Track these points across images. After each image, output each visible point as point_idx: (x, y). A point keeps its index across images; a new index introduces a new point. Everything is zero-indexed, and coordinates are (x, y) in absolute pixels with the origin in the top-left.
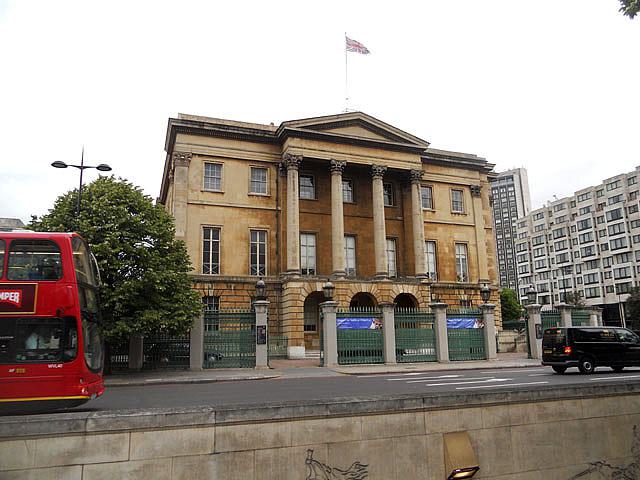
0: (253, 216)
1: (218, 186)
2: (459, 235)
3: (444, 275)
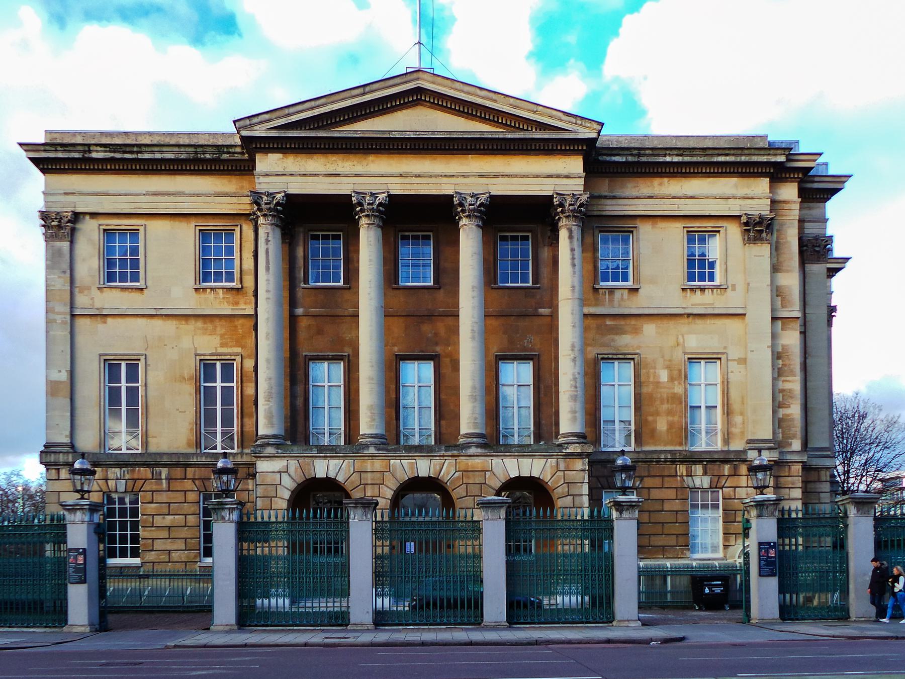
0: (205, 331)
1: (135, 277)
3: (653, 431)
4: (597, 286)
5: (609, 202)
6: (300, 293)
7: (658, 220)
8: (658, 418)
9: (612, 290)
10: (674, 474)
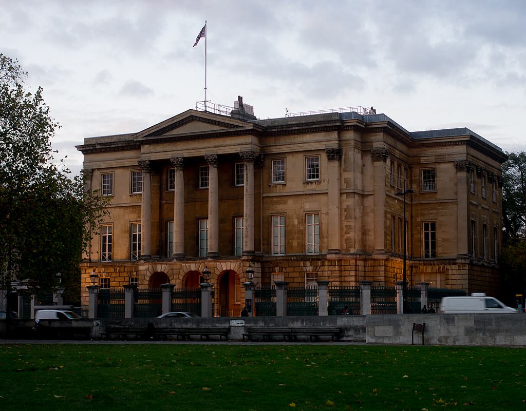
2: (308, 205)
3: (292, 246)
4: (270, 184)
5: (274, 147)
6: (164, 194)
7: (294, 153)
8: (294, 241)
9: (276, 185)
10: (298, 265)
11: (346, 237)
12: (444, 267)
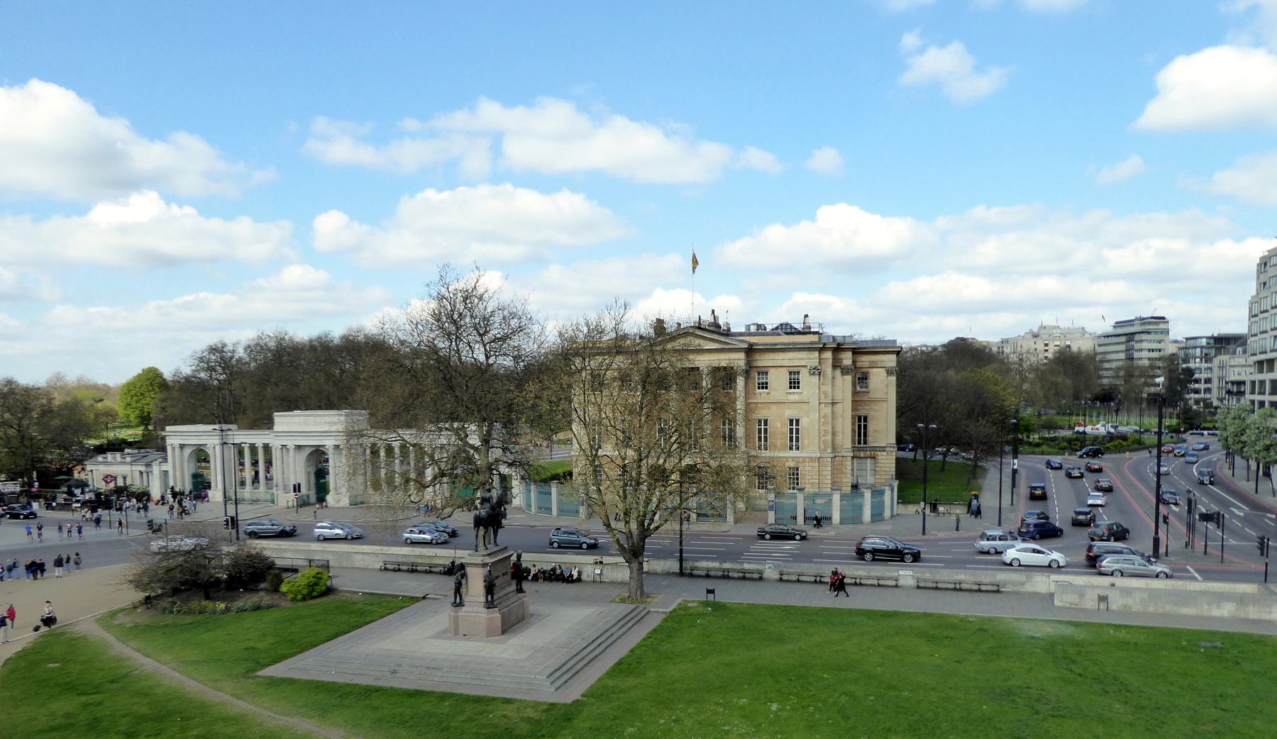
9: (760, 394)
11: (823, 438)
12: (874, 453)
